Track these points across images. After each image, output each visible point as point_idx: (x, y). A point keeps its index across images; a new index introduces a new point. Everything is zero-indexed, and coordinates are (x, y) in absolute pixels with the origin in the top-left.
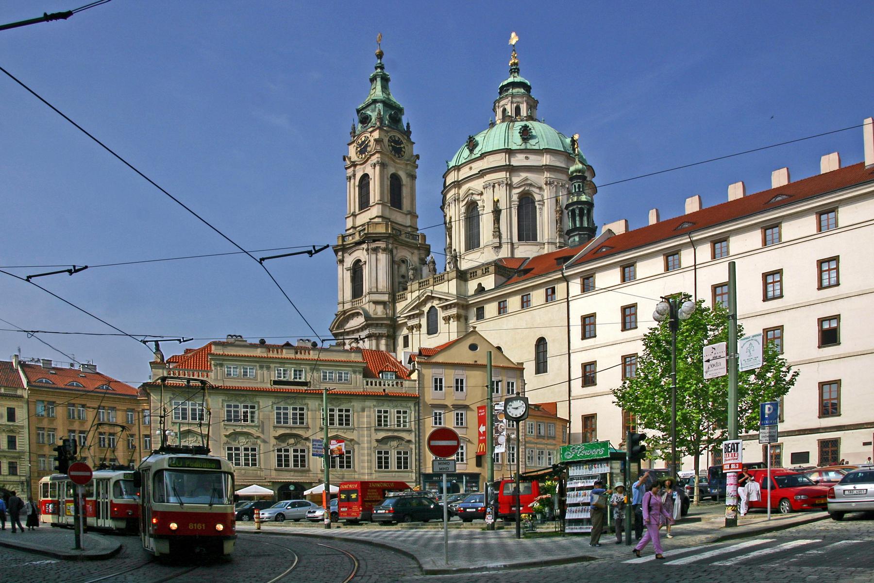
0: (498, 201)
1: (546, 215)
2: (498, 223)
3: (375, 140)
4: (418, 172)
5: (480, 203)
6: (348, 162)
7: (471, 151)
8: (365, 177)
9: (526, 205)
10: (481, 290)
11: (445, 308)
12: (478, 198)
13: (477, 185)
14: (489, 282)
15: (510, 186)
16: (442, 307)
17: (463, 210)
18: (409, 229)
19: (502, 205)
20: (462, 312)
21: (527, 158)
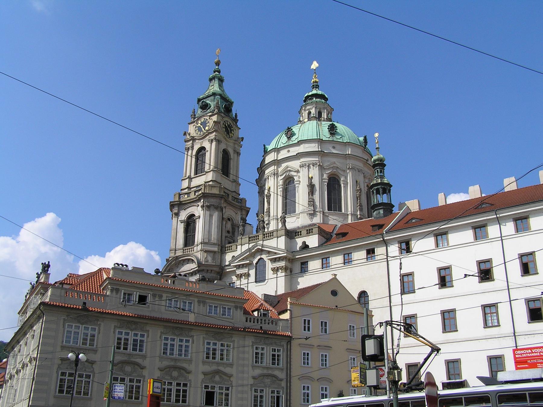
0: (312, 177)
3: (214, 122)
4: (242, 151)
5: (296, 178)
6: (188, 137)
8: (202, 149)
9: (333, 185)
10: (305, 247)
11: (274, 260)
12: (295, 174)
13: (295, 164)
14: (313, 241)
15: (322, 168)
16: (271, 260)
17: (281, 182)
18: (234, 194)
19: (316, 182)
20: (289, 265)
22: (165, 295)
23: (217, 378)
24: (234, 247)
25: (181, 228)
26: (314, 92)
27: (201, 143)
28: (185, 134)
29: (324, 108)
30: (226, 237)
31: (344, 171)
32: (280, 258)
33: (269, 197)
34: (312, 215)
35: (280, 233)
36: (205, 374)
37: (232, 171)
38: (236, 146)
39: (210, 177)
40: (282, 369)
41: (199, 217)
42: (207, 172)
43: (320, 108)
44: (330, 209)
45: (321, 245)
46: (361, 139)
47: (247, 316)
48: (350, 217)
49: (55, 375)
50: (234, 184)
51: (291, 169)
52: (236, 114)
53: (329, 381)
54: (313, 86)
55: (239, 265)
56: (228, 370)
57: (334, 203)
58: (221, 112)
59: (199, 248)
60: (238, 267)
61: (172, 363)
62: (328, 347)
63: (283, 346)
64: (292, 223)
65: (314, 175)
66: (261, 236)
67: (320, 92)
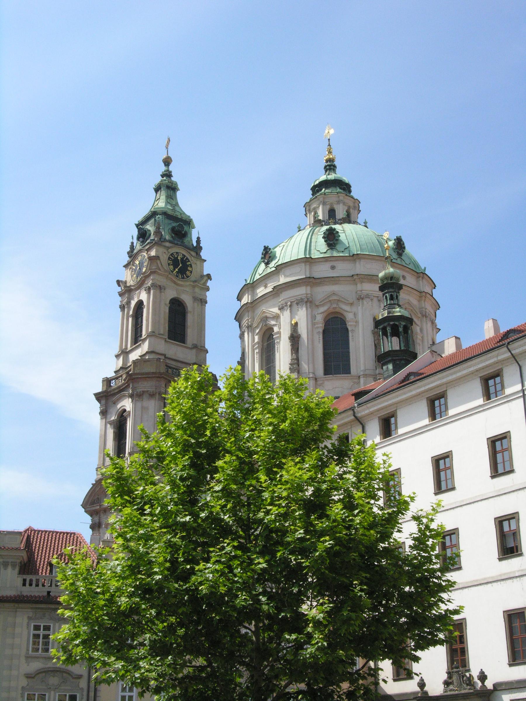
0: (296, 324)
1: (361, 340)
5: (276, 329)
7: (267, 264)
8: (140, 304)
12: (273, 322)
19: (303, 331)
21: (333, 268)
25: (111, 433)
27: (139, 297)
29: (338, 202)
31: (352, 304)
38: (197, 290)
43: (331, 204)
44: (327, 371)
47: (25, 577)
48: (362, 380)
50: (194, 351)
51: (268, 315)
52: (198, 238)
54: (325, 167)
58: (165, 240)
65: (300, 319)
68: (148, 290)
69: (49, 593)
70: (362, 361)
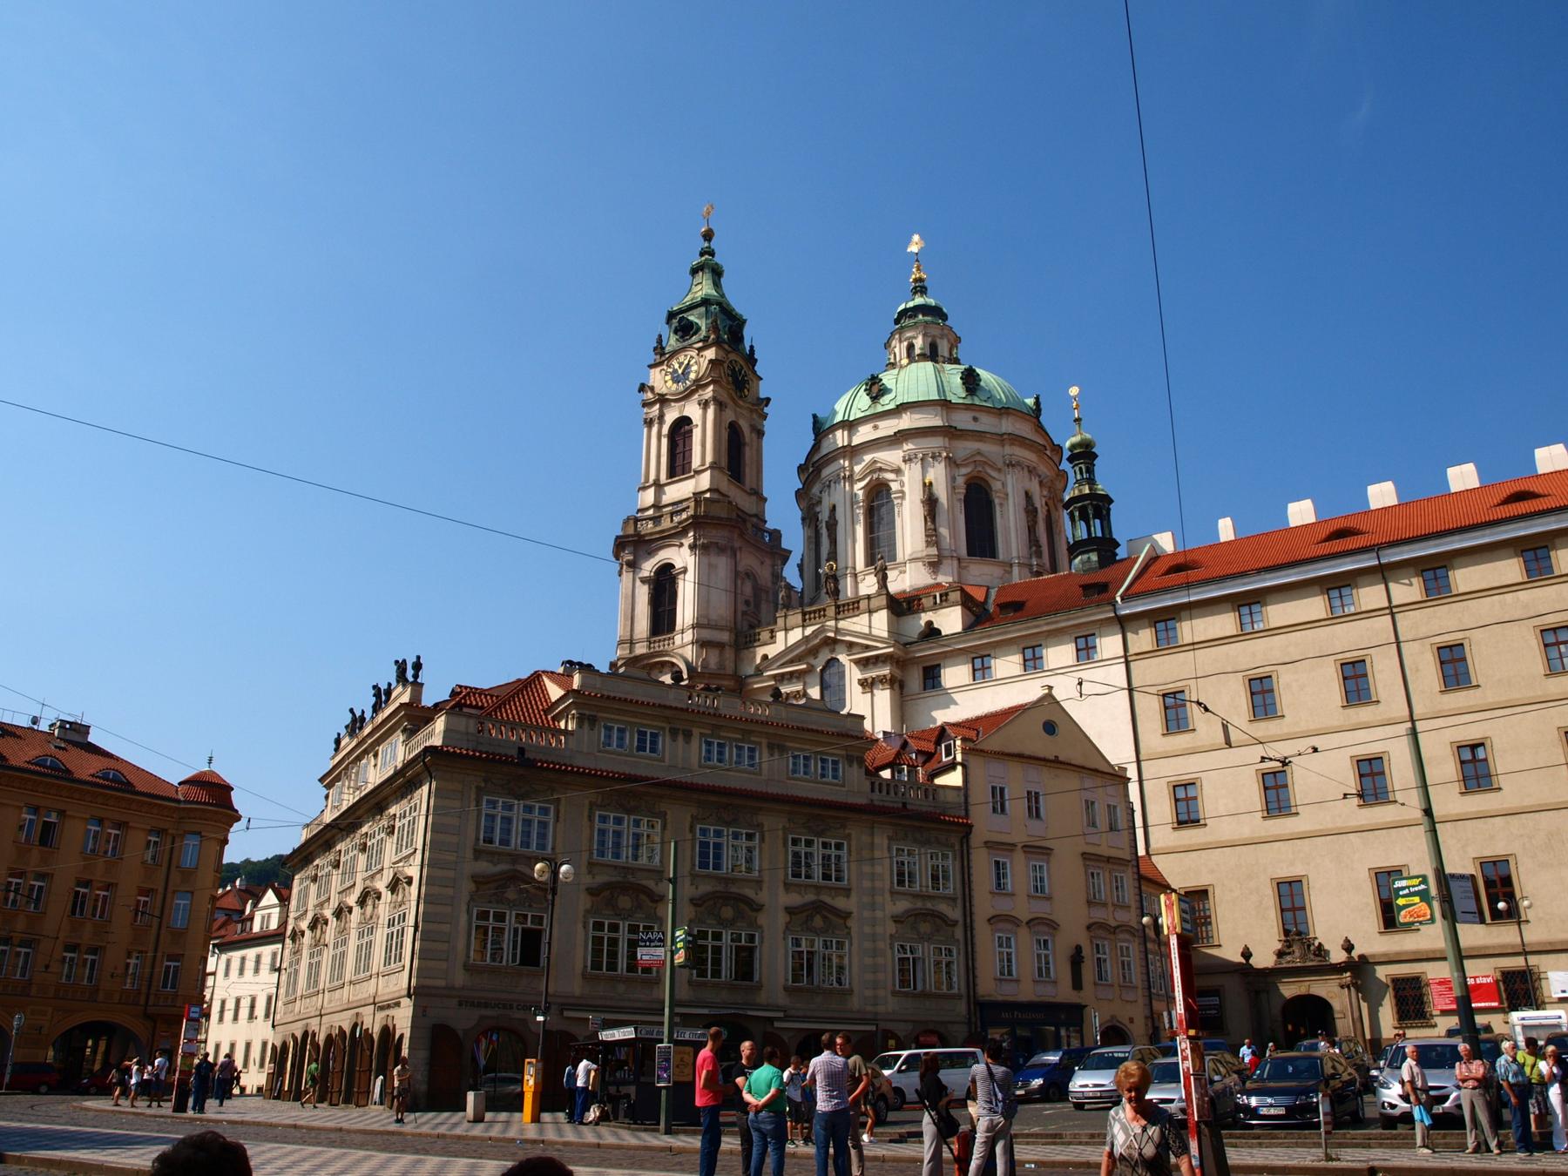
1: (1012, 518)
2: (934, 521)
3: (711, 361)
4: (768, 425)
5: (894, 486)
6: (650, 395)
8: (683, 424)
9: (978, 503)
10: (931, 632)
13: (892, 457)
14: (950, 620)
15: (951, 462)
16: (857, 662)
19: (941, 492)
20: (898, 673)
21: (975, 419)
22: (696, 732)
23: (818, 921)
24: (765, 635)
25: (643, 592)
26: (919, 300)
28: (642, 388)
29: (942, 337)
30: (744, 613)
31: (999, 470)
32: (877, 657)
33: (832, 525)
34: (934, 566)
35: (874, 603)
36: (790, 911)
37: (748, 471)
39: (704, 481)
40: (954, 900)
41: (685, 571)
42: (698, 472)
45: (968, 628)
46: (1030, 401)
48: (1016, 570)
49: (464, 918)
50: (754, 498)
53: (1053, 925)
55: (783, 675)
56: (840, 903)
57: (981, 541)
59: (688, 636)
60: (781, 678)
61: (720, 888)
62: (1046, 852)
63: (953, 846)
64: (900, 582)
66: (831, 611)
67: (932, 302)
68: (705, 405)
69: (904, 804)
70: (1014, 546)
